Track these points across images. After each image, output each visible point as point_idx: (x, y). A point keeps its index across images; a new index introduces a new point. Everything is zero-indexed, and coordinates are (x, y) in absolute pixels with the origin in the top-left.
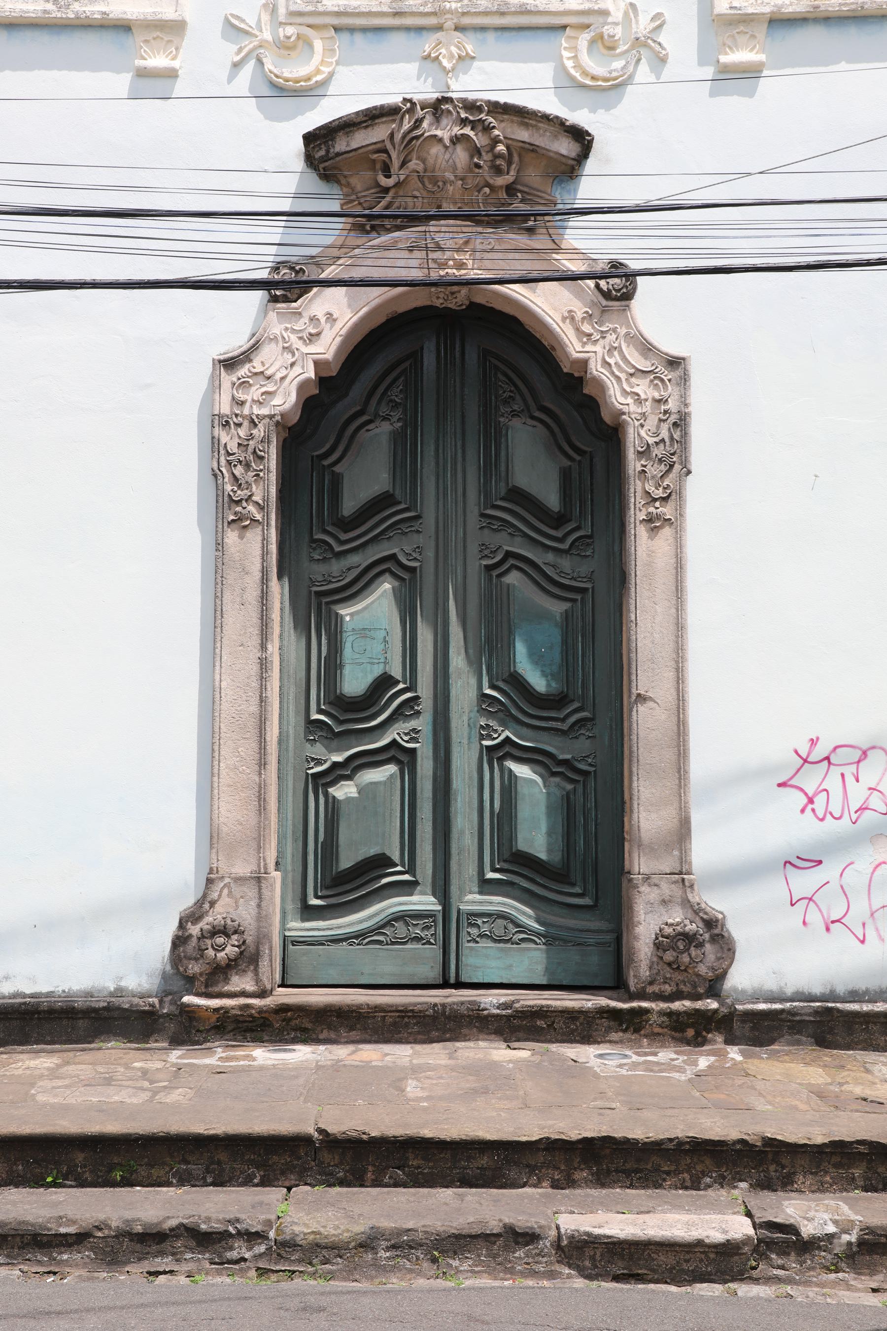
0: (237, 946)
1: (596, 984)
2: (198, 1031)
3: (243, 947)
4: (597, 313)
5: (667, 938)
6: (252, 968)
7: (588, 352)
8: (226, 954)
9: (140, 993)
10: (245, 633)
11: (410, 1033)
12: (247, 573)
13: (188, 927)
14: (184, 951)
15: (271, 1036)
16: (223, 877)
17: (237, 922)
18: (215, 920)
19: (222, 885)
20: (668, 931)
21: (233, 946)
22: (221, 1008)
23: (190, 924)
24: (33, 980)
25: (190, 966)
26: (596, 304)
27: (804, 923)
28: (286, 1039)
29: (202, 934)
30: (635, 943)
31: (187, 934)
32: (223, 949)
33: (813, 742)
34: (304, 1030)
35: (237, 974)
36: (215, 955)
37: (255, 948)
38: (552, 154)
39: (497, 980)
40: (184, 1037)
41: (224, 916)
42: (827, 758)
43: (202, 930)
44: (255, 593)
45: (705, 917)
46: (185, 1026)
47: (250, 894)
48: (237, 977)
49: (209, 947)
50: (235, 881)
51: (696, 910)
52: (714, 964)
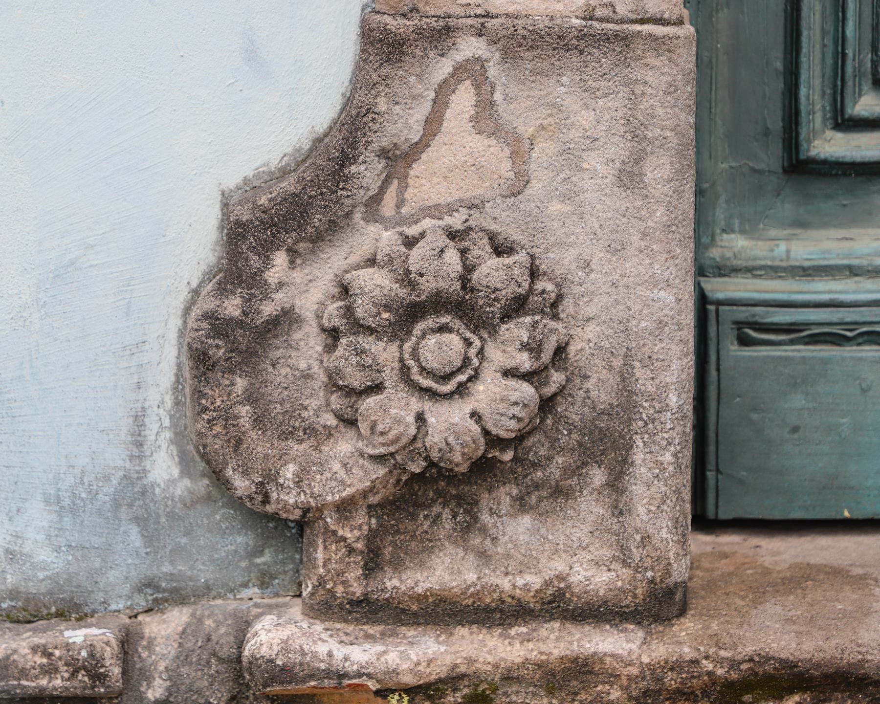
0: (527, 377)
3: (557, 378)
6: (598, 476)
8: (475, 415)
13: (273, 276)
14: (251, 397)
16: (448, 30)
17: (521, 257)
18: (410, 243)
19: (444, 68)
21: (509, 373)
22: (453, 680)
23: (280, 258)
25: (290, 471)
29: (349, 311)
31: (268, 309)
32: (461, 391)
35: (521, 504)
36: (420, 418)
37: (613, 380)
41: (456, 221)
43: (345, 290)
47: (586, 119)
48: (526, 520)
49: (389, 376)
50: (507, 55)
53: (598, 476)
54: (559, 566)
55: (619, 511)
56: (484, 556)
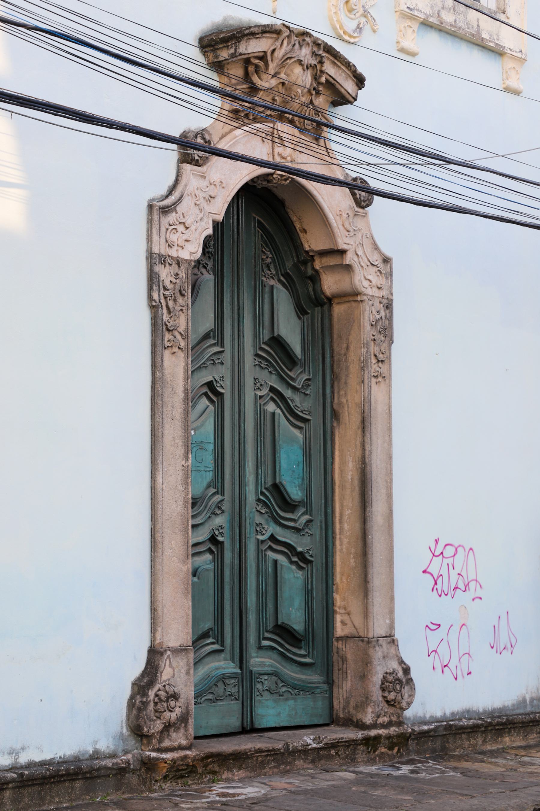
1: (321, 722)
2: (156, 781)
4: (351, 215)
5: (391, 683)
7: (348, 244)
9: (108, 753)
10: (174, 443)
11: (270, 768)
12: (174, 393)
15: (193, 780)
20: (390, 678)
24: (40, 749)
26: (352, 209)
27: (434, 668)
28: (205, 781)
30: (373, 688)
33: (437, 541)
34: (214, 773)
35: (174, 731)
38: (343, 90)
39: (273, 725)
40: (142, 788)
42: (442, 553)
44: (180, 410)
45: (404, 667)
46: (143, 779)
48: (175, 733)
51: (401, 662)
52: (409, 700)
53: (183, 725)
54: (179, 741)
55: (186, 731)
56: (170, 740)
